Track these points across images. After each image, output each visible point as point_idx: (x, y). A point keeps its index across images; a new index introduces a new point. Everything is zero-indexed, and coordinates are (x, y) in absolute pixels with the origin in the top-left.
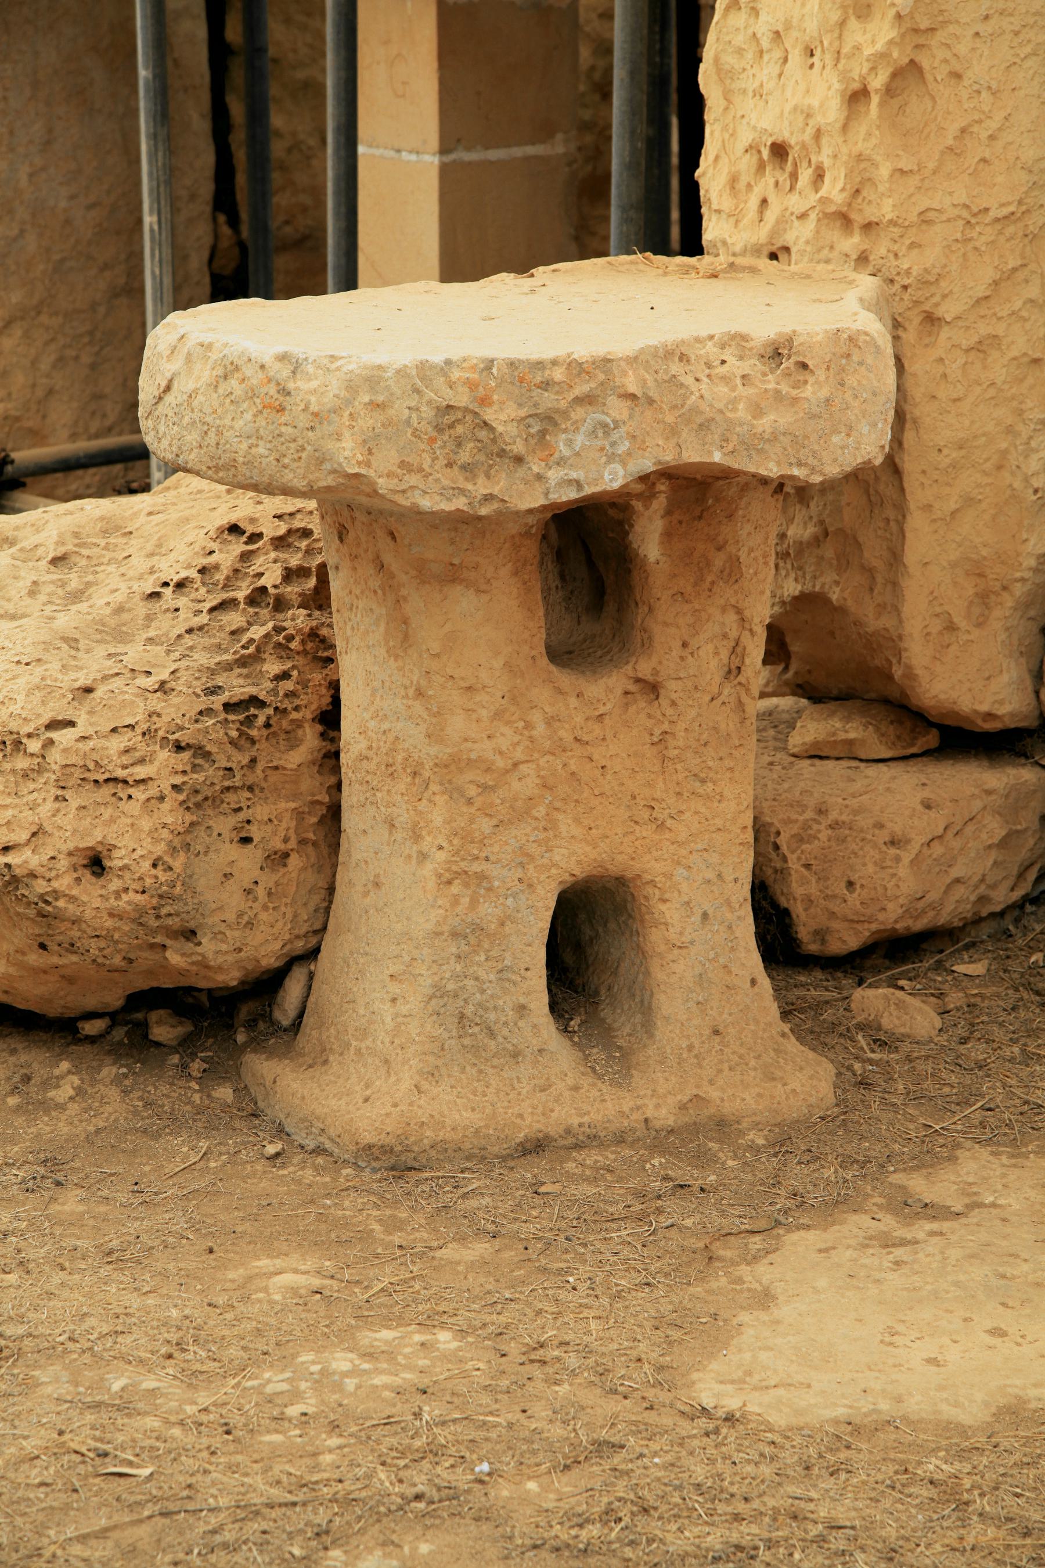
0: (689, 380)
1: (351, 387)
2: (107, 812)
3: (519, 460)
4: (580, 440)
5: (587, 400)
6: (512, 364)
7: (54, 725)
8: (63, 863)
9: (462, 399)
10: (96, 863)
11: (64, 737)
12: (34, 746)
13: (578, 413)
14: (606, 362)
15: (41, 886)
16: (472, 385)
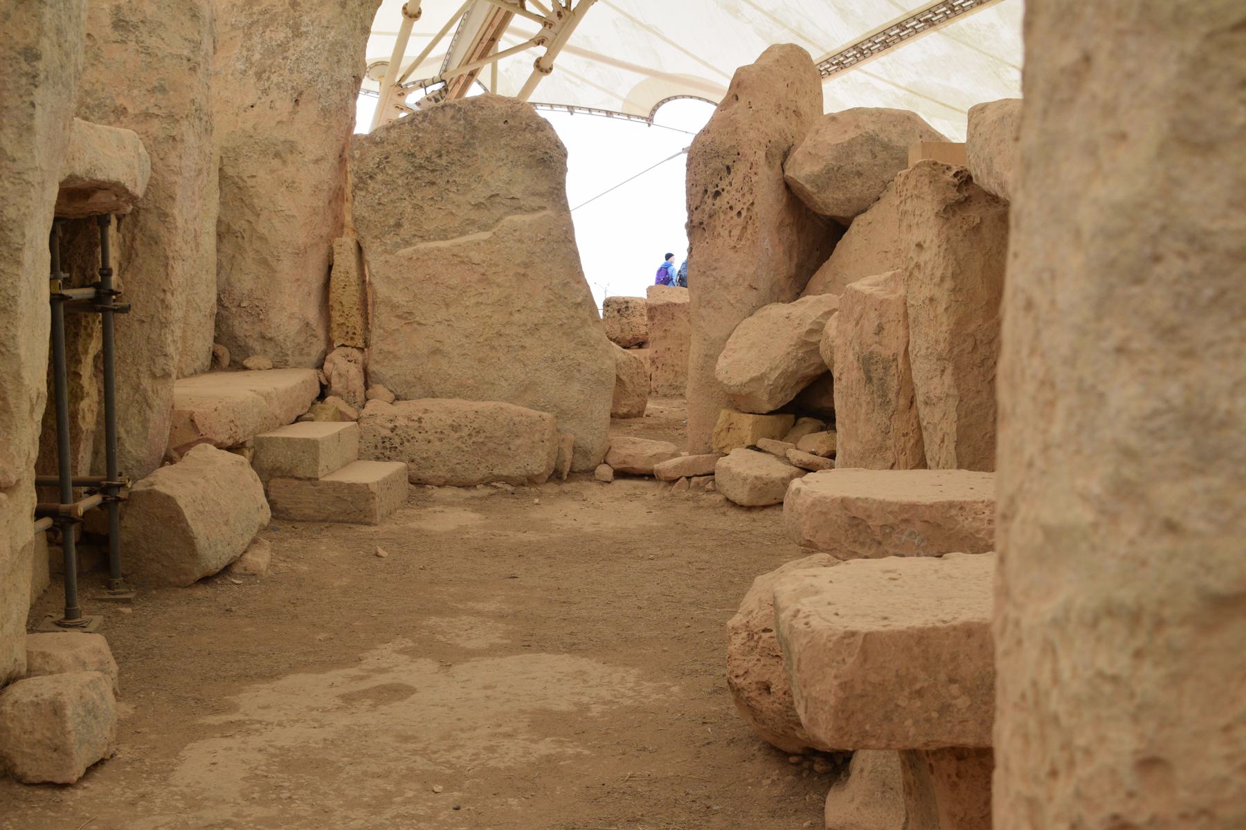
0: (961, 519)
1: (813, 504)
2: (773, 668)
3: (880, 543)
4: (904, 537)
5: (906, 521)
6: (881, 502)
7: (765, 630)
8: (754, 686)
9: (860, 515)
10: (767, 688)
11: (766, 636)
12: (756, 637)
13: (903, 526)
14: (913, 506)
15: (746, 694)
16: (866, 510)
